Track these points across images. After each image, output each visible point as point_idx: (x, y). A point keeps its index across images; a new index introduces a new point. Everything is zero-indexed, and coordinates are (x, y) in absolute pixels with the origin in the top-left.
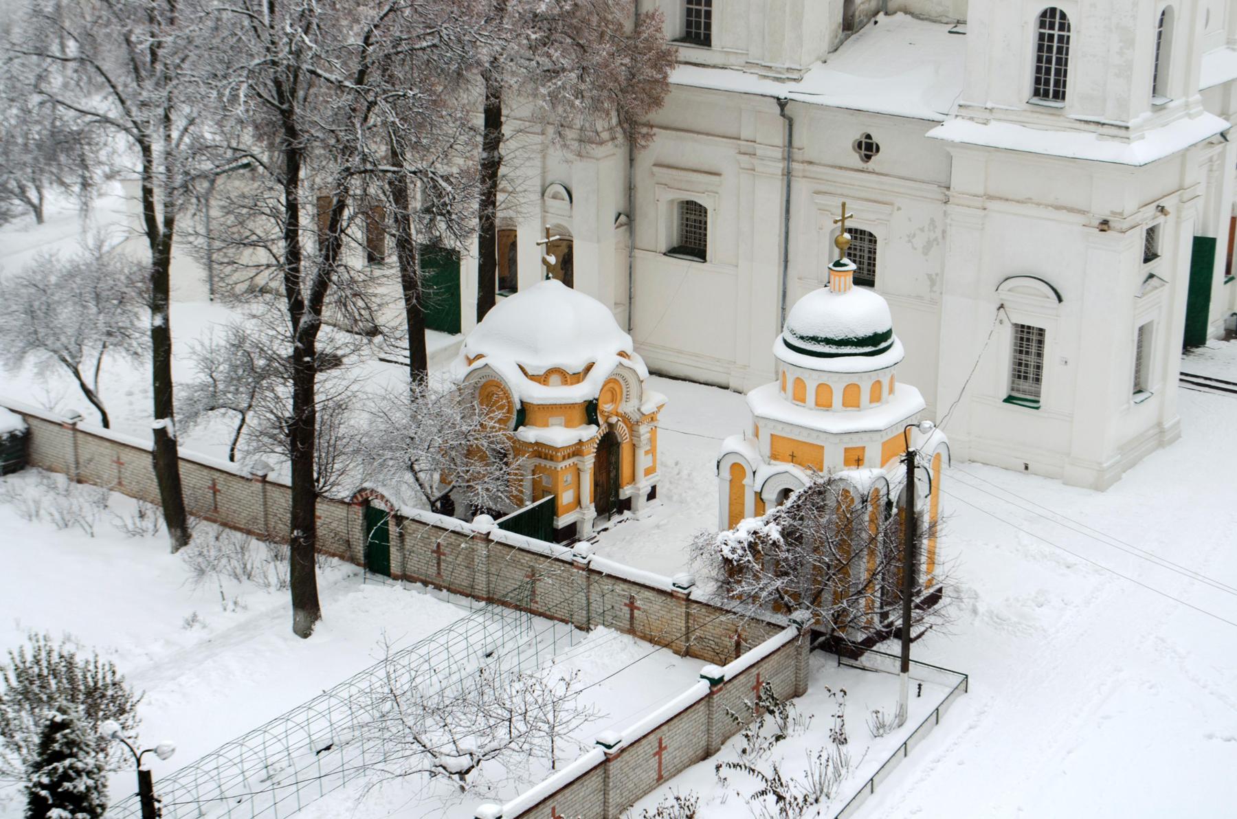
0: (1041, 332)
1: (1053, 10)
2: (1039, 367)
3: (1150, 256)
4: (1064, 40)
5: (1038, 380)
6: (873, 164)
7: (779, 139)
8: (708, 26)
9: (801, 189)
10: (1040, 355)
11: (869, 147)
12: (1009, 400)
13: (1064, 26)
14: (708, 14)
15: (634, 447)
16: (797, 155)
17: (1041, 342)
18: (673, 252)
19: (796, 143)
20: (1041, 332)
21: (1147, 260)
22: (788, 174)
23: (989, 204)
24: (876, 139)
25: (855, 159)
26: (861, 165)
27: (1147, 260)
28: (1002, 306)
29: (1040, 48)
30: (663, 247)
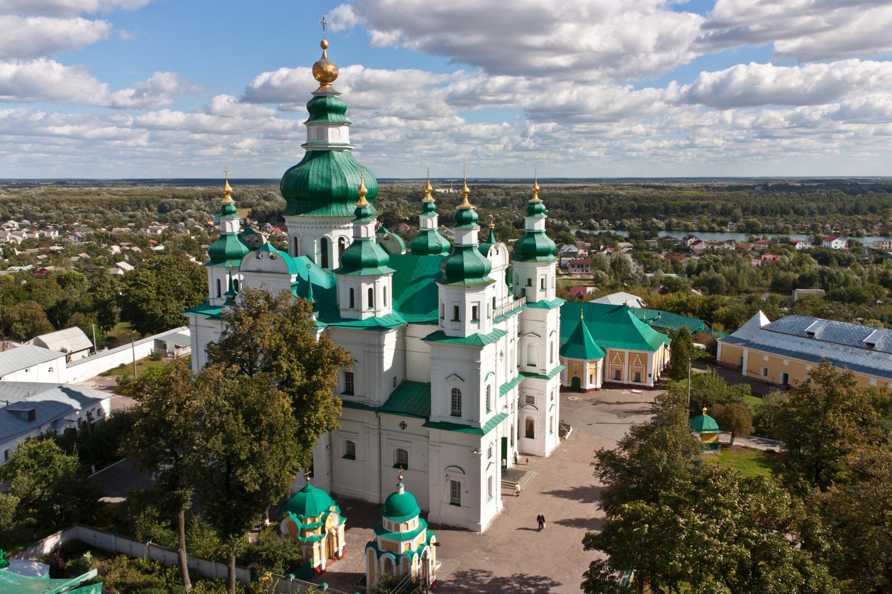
0: (459, 483)
1: (456, 389)
2: (459, 493)
3: (490, 456)
4: (460, 397)
5: (459, 497)
6: (406, 430)
7: (376, 423)
8: (353, 388)
9: (384, 438)
10: (459, 489)
11: (404, 425)
12: (452, 504)
13: (459, 393)
14: (353, 384)
15: (337, 536)
16: (382, 428)
17: (459, 485)
18: (345, 457)
19: (382, 424)
20: (459, 483)
21: (489, 458)
22: (380, 433)
23: (441, 444)
24: (406, 423)
25: (400, 429)
26: (401, 430)
27: (489, 458)
28: (447, 475)
29: (453, 399)
30: (342, 455)
